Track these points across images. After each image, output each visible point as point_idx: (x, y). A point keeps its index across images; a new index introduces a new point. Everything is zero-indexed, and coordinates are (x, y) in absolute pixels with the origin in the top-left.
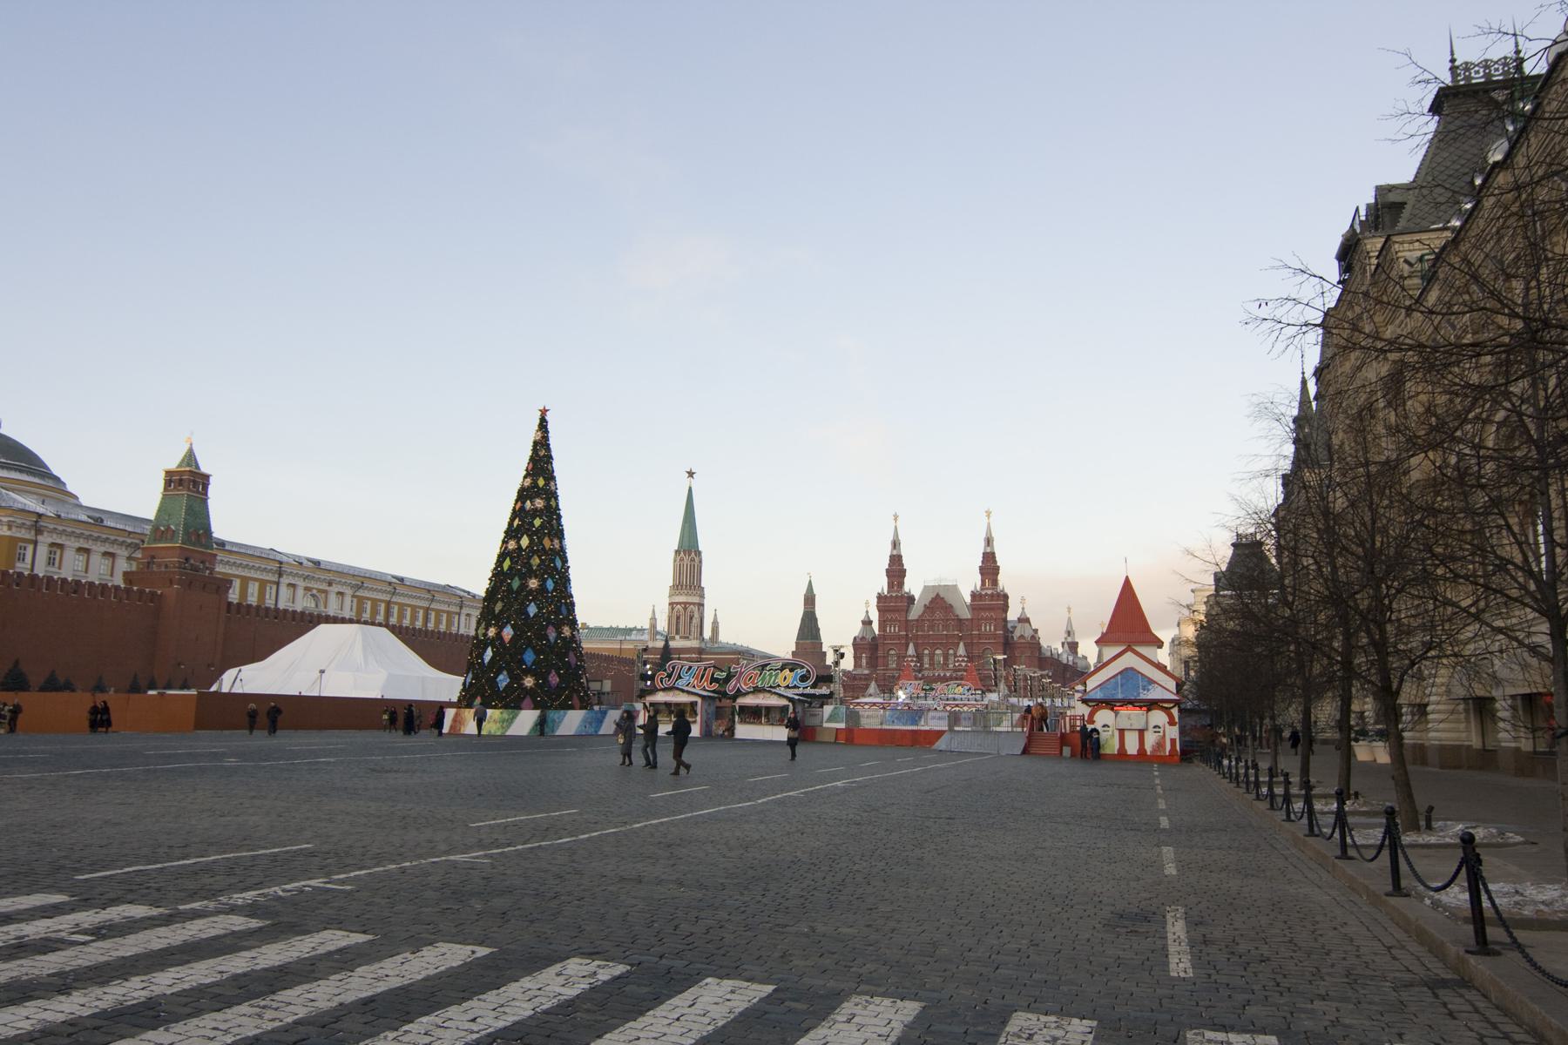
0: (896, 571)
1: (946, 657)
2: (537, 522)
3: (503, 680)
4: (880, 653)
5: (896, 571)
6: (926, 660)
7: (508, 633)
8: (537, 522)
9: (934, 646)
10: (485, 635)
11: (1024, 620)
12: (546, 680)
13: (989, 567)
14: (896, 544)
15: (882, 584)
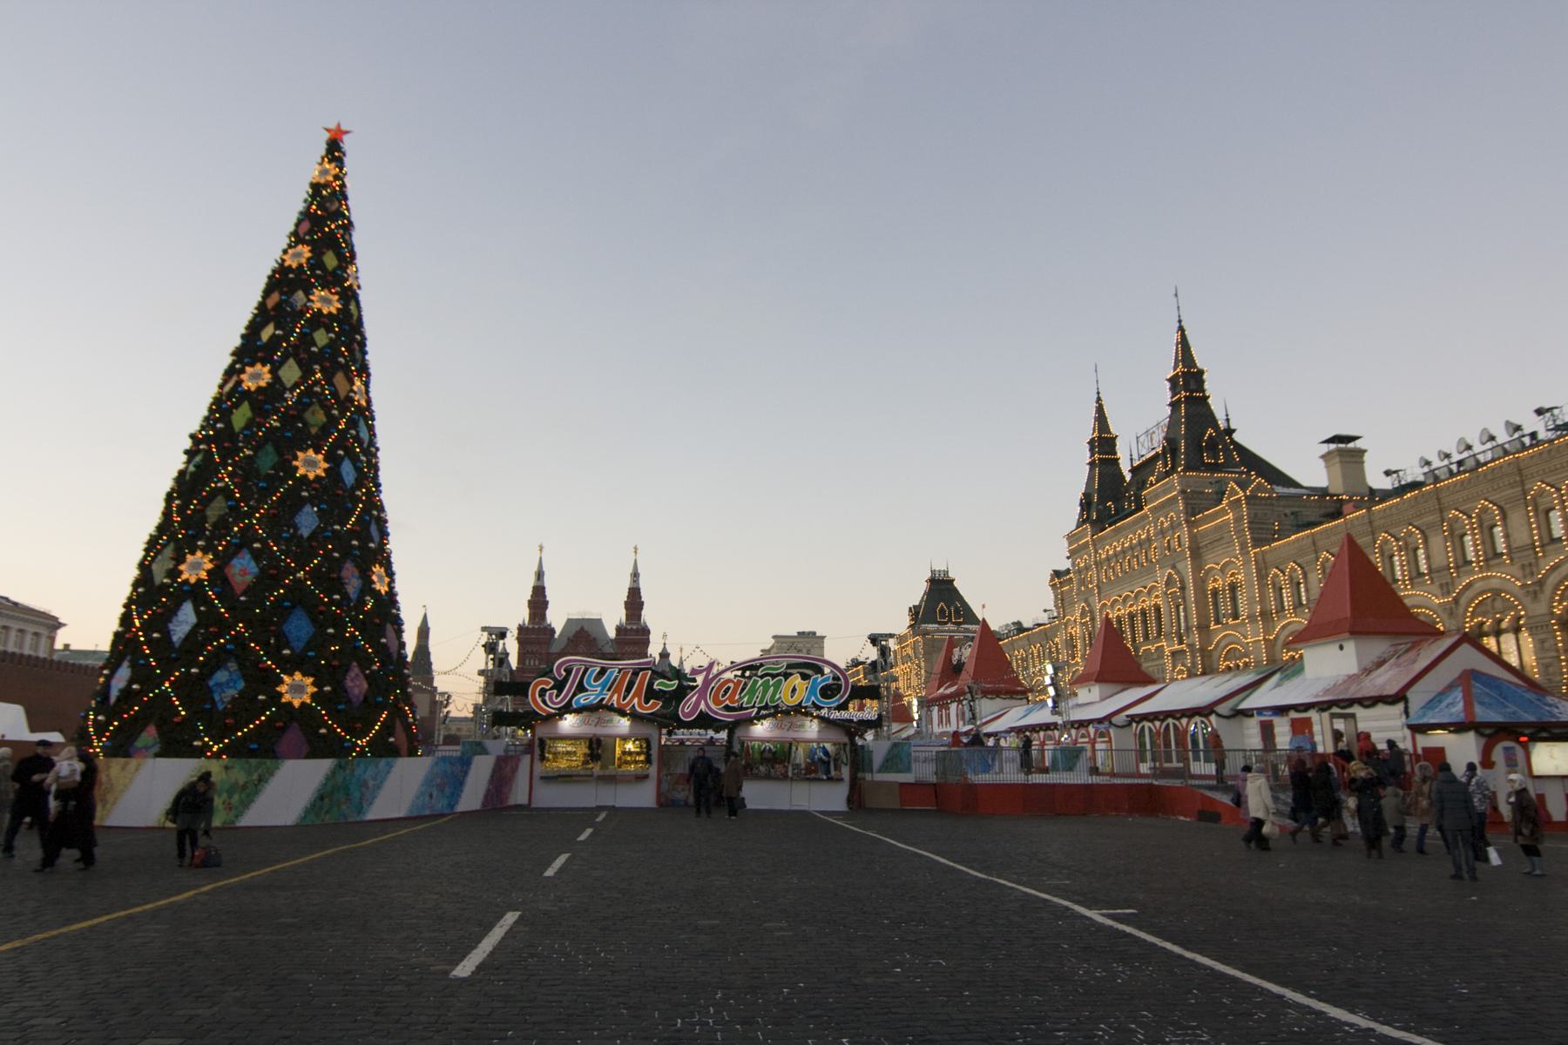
0: (538, 602)
2: (321, 338)
3: (227, 684)
5: (538, 602)
7: (243, 569)
8: (321, 338)
10: (174, 573)
11: (664, 655)
12: (340, 689)
14: (540, 575)
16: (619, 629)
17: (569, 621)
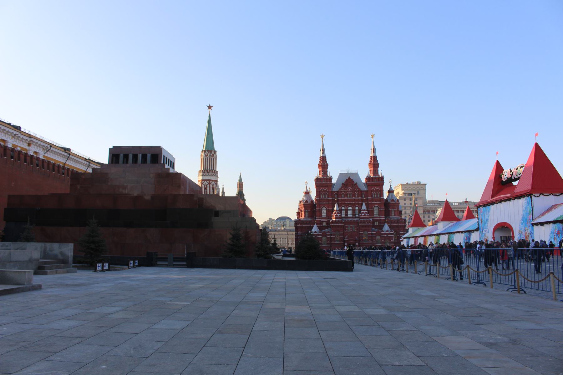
0: (324, 164)
1: (354, 211)
4: (317, 209)
5: (324, 164)
6: (343, 212)
9: (347, 205)
11: (391, 192)
13: (375, 164)
15: (316, 172)
16: (368, 179)
17: (341, 175)
